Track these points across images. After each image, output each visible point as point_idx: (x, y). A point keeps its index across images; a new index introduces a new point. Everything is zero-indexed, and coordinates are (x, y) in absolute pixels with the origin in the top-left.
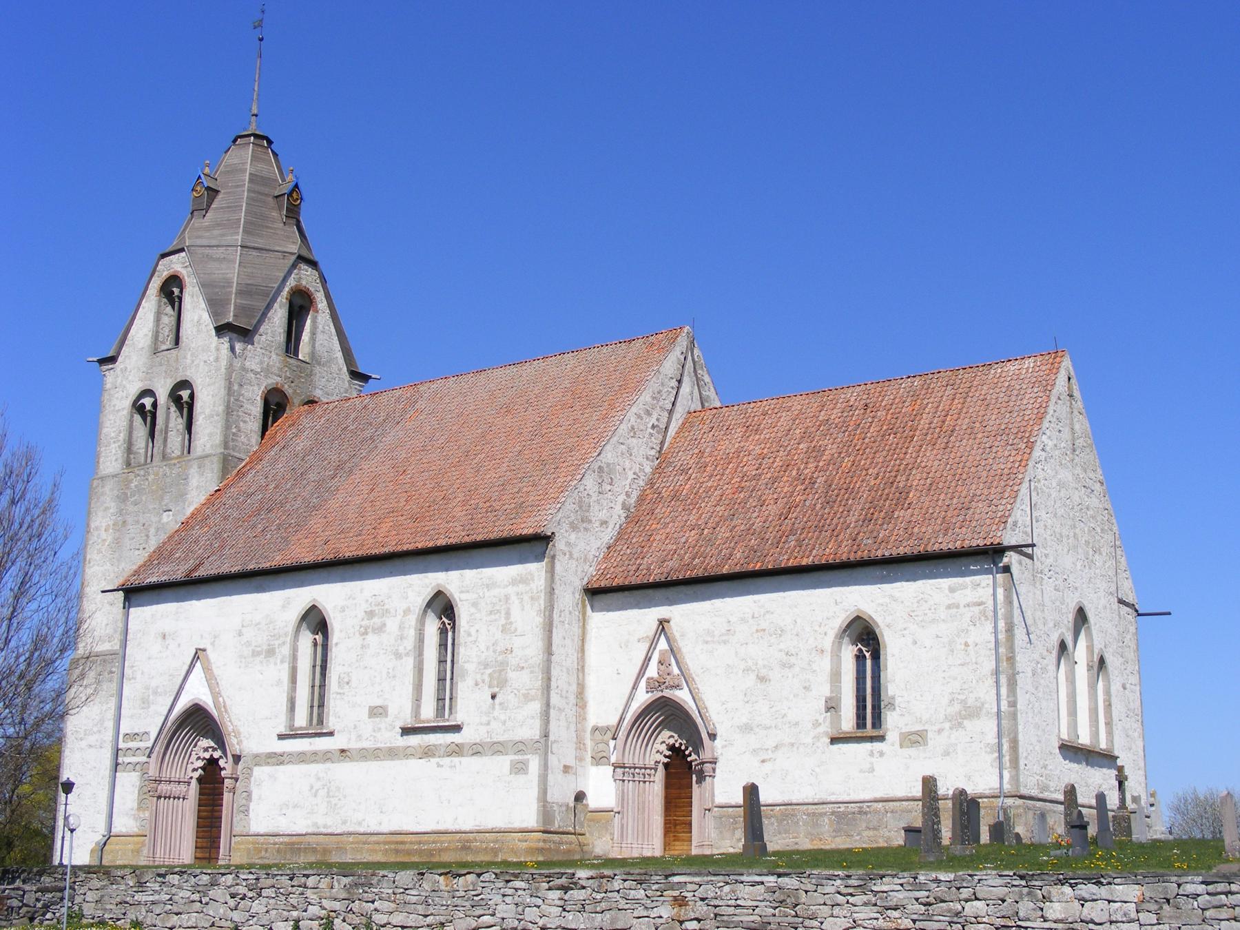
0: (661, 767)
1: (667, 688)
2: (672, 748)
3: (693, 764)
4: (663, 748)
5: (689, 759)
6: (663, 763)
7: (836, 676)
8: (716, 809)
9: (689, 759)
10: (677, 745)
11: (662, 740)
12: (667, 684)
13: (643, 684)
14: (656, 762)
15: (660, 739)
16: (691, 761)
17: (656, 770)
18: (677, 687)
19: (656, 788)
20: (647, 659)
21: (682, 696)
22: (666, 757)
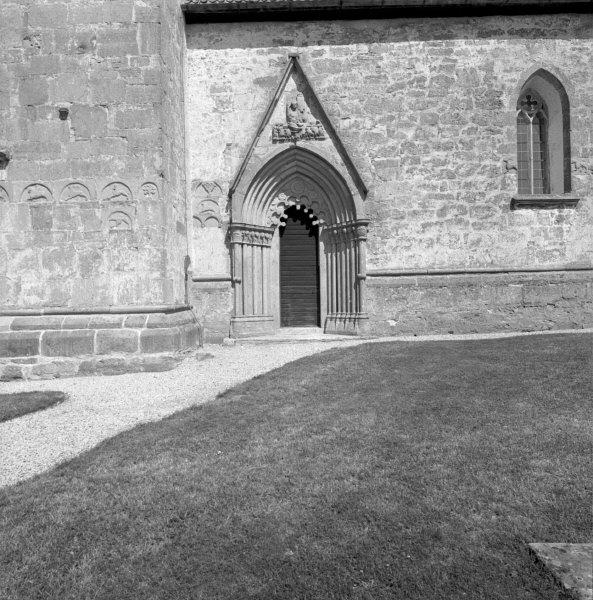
0: (277, 231)
1: (302, 137)
2: (290, 211)
3: (321, 229)
4: (281, 210)
5: (314, 223)
6: (281, 228)
7: (522, 143)
8: (368, 278)
9: (314, 223)
10: (298, 207)
11: (279, 201)
12: (304, 132)
13: (268, 132)
14: (273, 225)
15: (276, 201)
16: (317, 226)
17: (273, 233)
18: (317, 136)
19: (272, 254)
20: (274, 103)
21: (325, 148)
22: (282, 220)
